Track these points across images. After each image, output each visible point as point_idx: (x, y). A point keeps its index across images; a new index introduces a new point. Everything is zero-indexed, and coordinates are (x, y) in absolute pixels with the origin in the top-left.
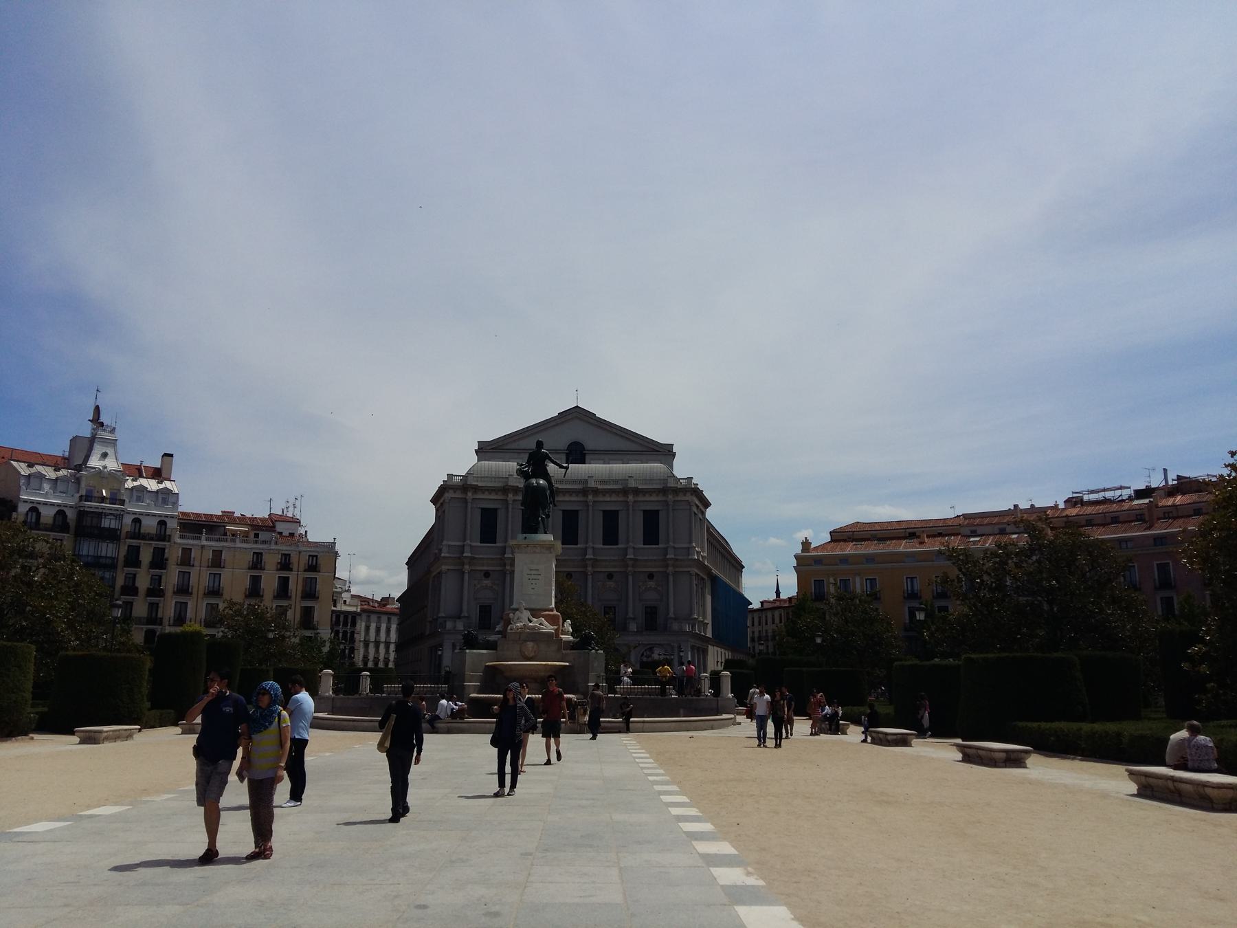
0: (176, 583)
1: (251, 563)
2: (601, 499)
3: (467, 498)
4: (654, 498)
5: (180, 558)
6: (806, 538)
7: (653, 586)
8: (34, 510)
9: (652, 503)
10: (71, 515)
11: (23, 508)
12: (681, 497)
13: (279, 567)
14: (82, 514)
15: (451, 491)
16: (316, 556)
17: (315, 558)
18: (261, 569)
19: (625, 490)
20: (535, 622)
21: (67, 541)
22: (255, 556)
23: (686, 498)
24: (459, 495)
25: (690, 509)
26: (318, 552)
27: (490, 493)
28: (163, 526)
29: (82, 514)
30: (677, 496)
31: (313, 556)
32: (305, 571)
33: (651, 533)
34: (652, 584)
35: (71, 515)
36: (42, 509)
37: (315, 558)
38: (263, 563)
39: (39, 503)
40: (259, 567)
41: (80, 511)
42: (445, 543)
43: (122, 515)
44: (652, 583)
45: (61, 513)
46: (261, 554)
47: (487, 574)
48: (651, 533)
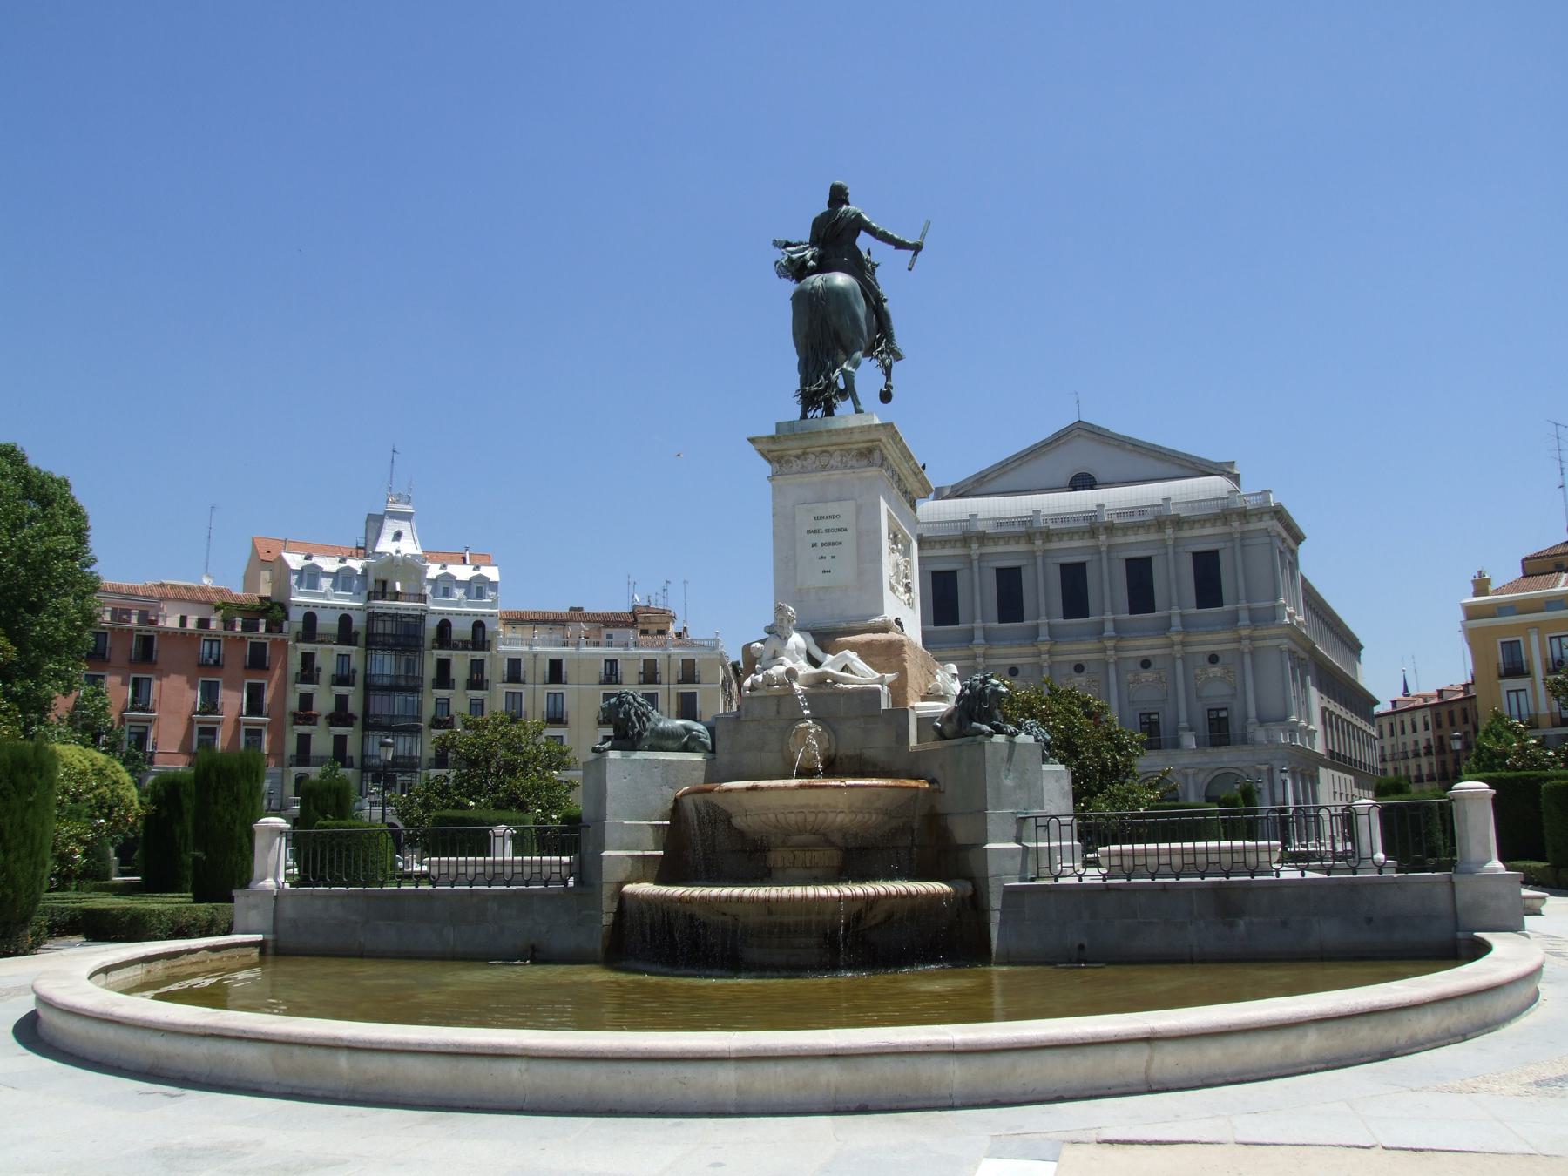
0: (546, 710)
1: (603, 674)
2: (1120, 540)
4: (1208, 531)
5: (506, 673)
6: (1480, 572)
7: (1219, 675)
8: (310, 619)
9: (1205, 537)
10: (358, 622)
11: (296, 616)
12: (1254, 525)
13: (642, 679)
14: (372, 617)
18: (617, 683)
19: (1163, 520)
21: (355, 653)
22: (608, 664)
25: (1271, 543)
26: (695, 654)
27: (943, 547)
28: (481, 629)
29: (372, 617)
30: (1248, 522)
32: (679, 682)
33: (1209, 587)
34: (1215, 670)
35: (358, 622)
36: (318, 613)
38: (619, 674)
39: (352, 609)
40: (614, 679)
41: (368, 613)
43: (424, 616)
45: (345, 621)
46: (616, 661)
48: (1209, 587)
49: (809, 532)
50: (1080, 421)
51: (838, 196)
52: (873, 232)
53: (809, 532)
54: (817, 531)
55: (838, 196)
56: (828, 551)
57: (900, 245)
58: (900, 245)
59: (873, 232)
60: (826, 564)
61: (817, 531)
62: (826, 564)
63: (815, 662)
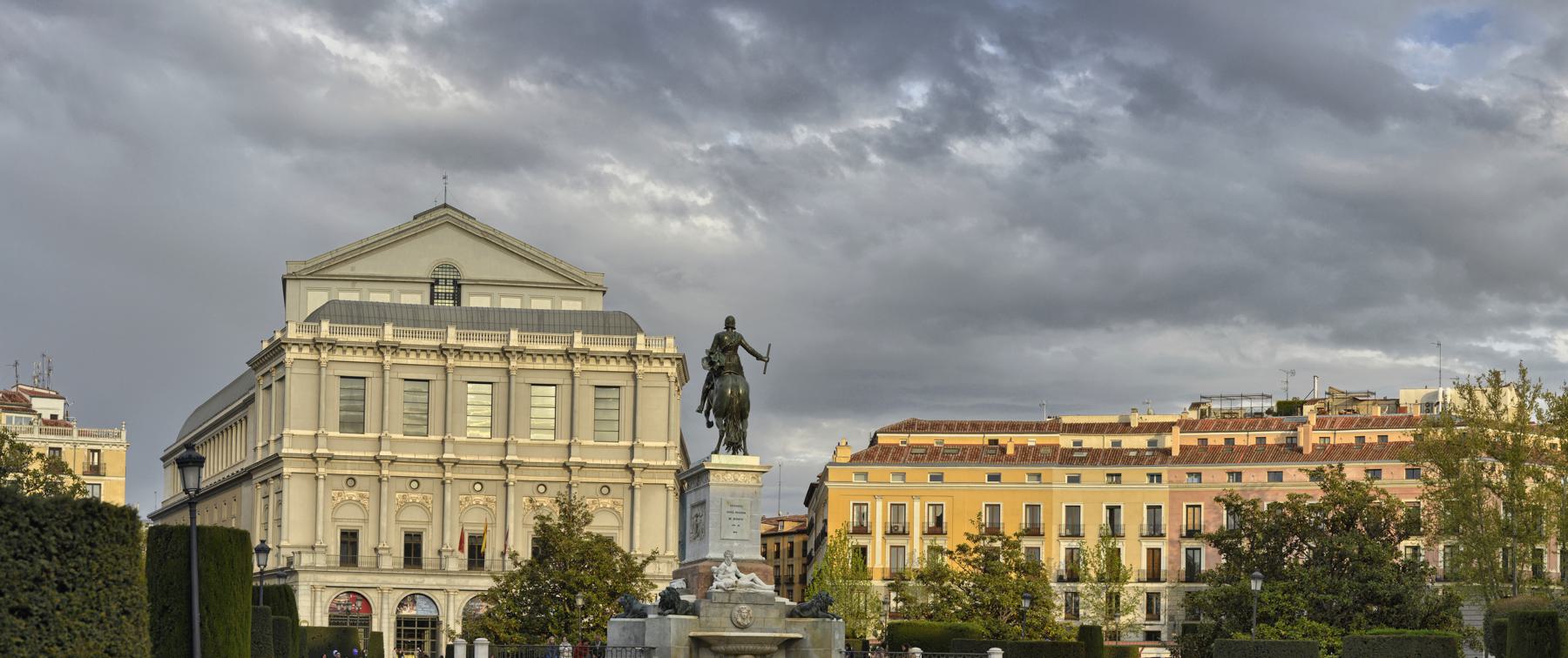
3: (574, 369)
7: (608, 506)
15: (295, 349)
16: (98, 451)
17: (96, 454)
20: (745, 579)
23: (664, 370)
24: (306, 353)
31: (93, 451)
37: (96, 454)
42: (286, 431)
44: (606, 501)
47: (352, 481)
49: (728, 512)
50: (445, 206)
51: (730, 324)
52: (745, 347)
53: (728, 512)
54: (732, 512)
55: (730, 324)
56: (736, 522)
57: (759, 357)
58: (759, 357)
59: (745, 347)
60: (735, 529)
61: (732, 512)
62: (735, 529)
63: (739, 578)
